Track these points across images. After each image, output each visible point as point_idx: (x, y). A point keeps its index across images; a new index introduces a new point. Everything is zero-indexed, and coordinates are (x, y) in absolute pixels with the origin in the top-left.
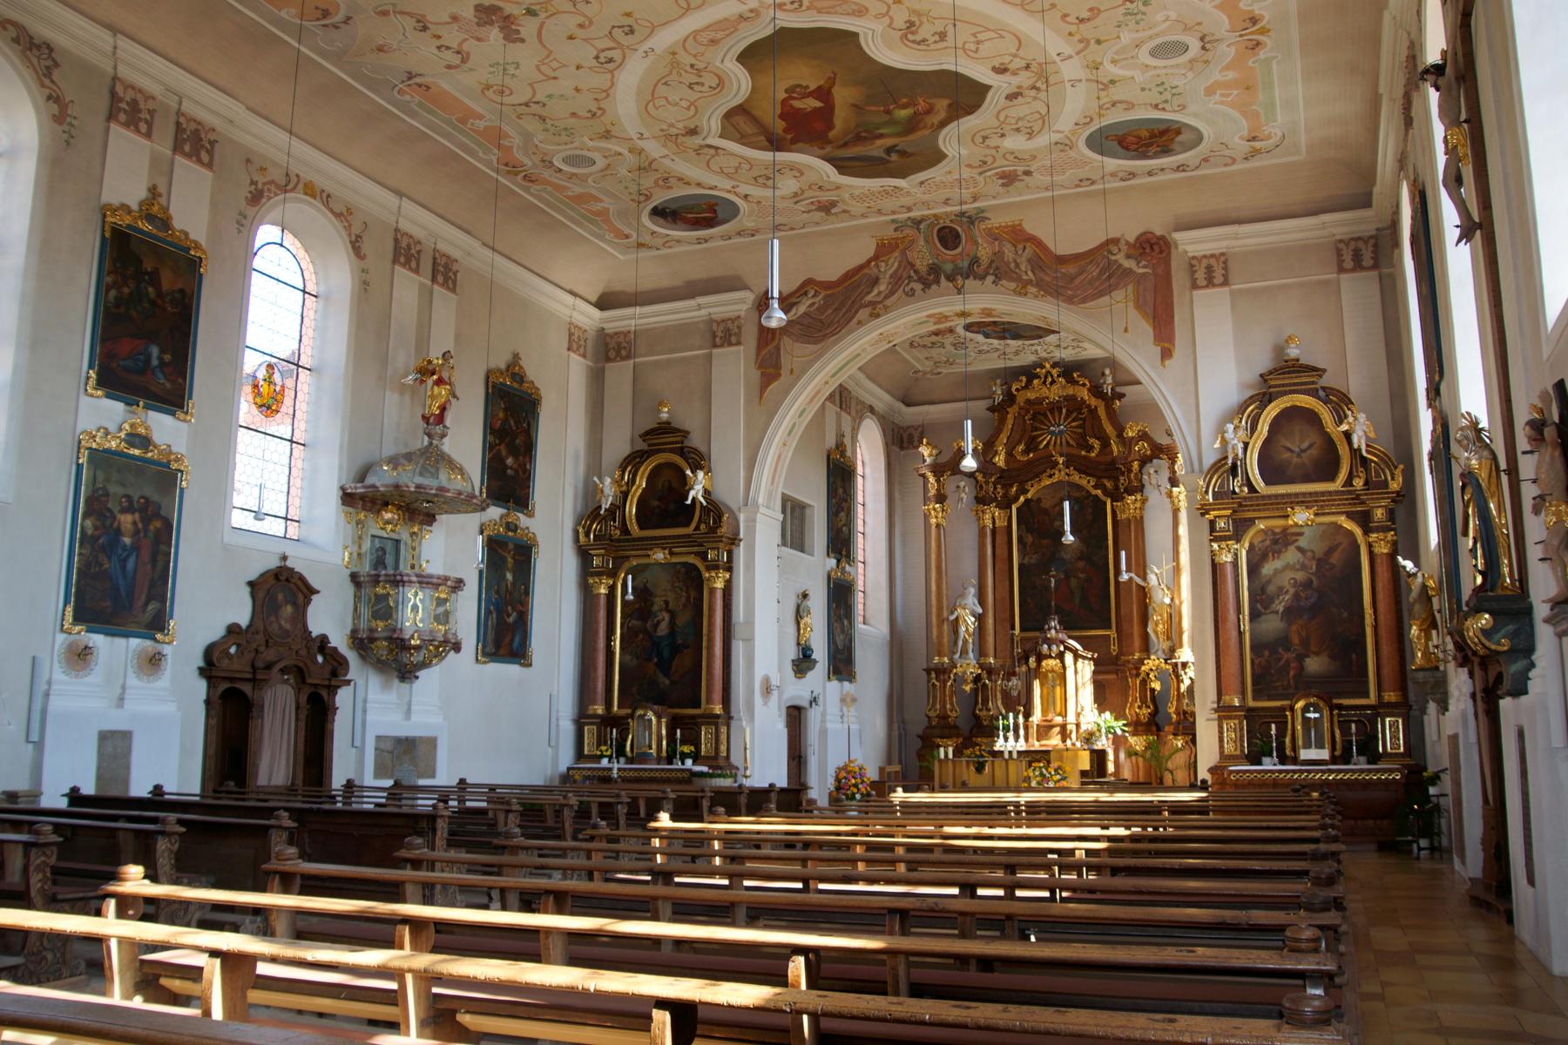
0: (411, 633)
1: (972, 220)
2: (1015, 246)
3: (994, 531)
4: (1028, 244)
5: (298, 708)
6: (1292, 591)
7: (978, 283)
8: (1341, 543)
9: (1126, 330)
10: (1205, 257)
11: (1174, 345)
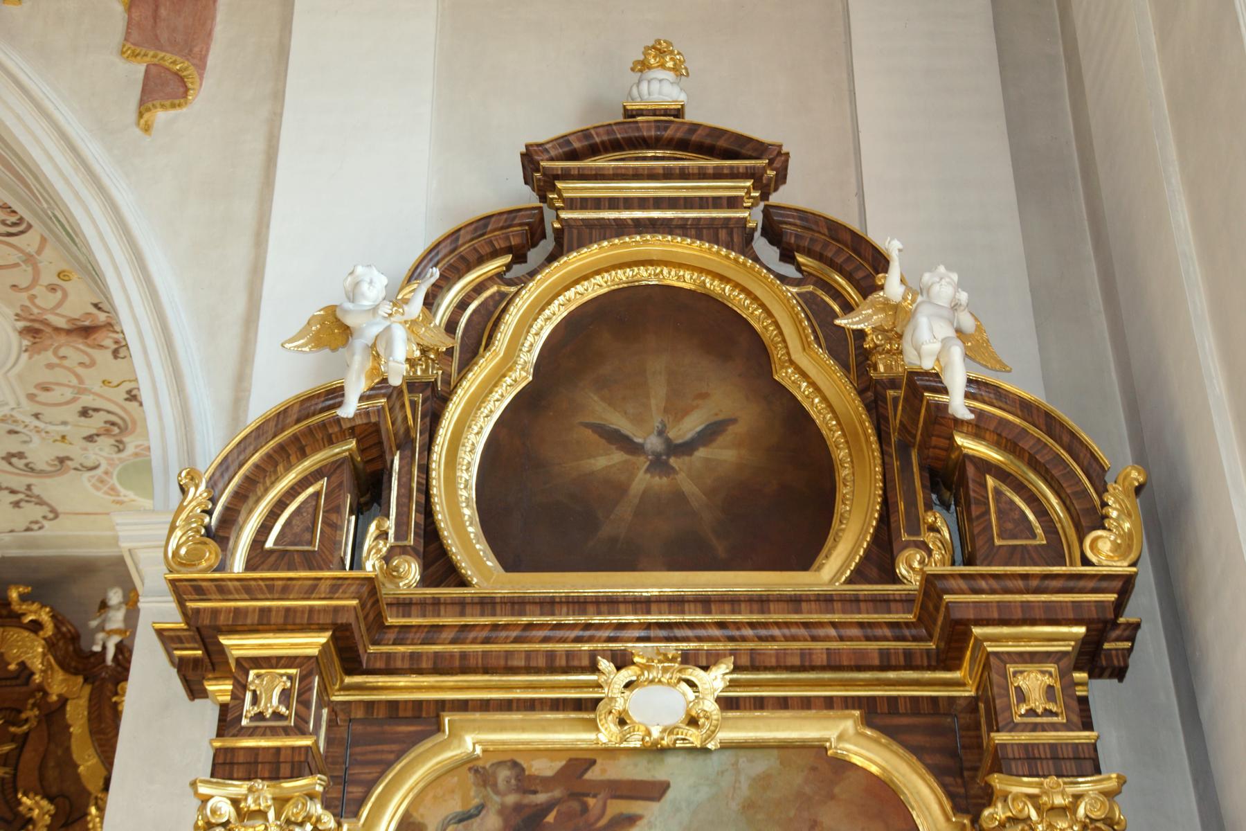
11: (201, 66)
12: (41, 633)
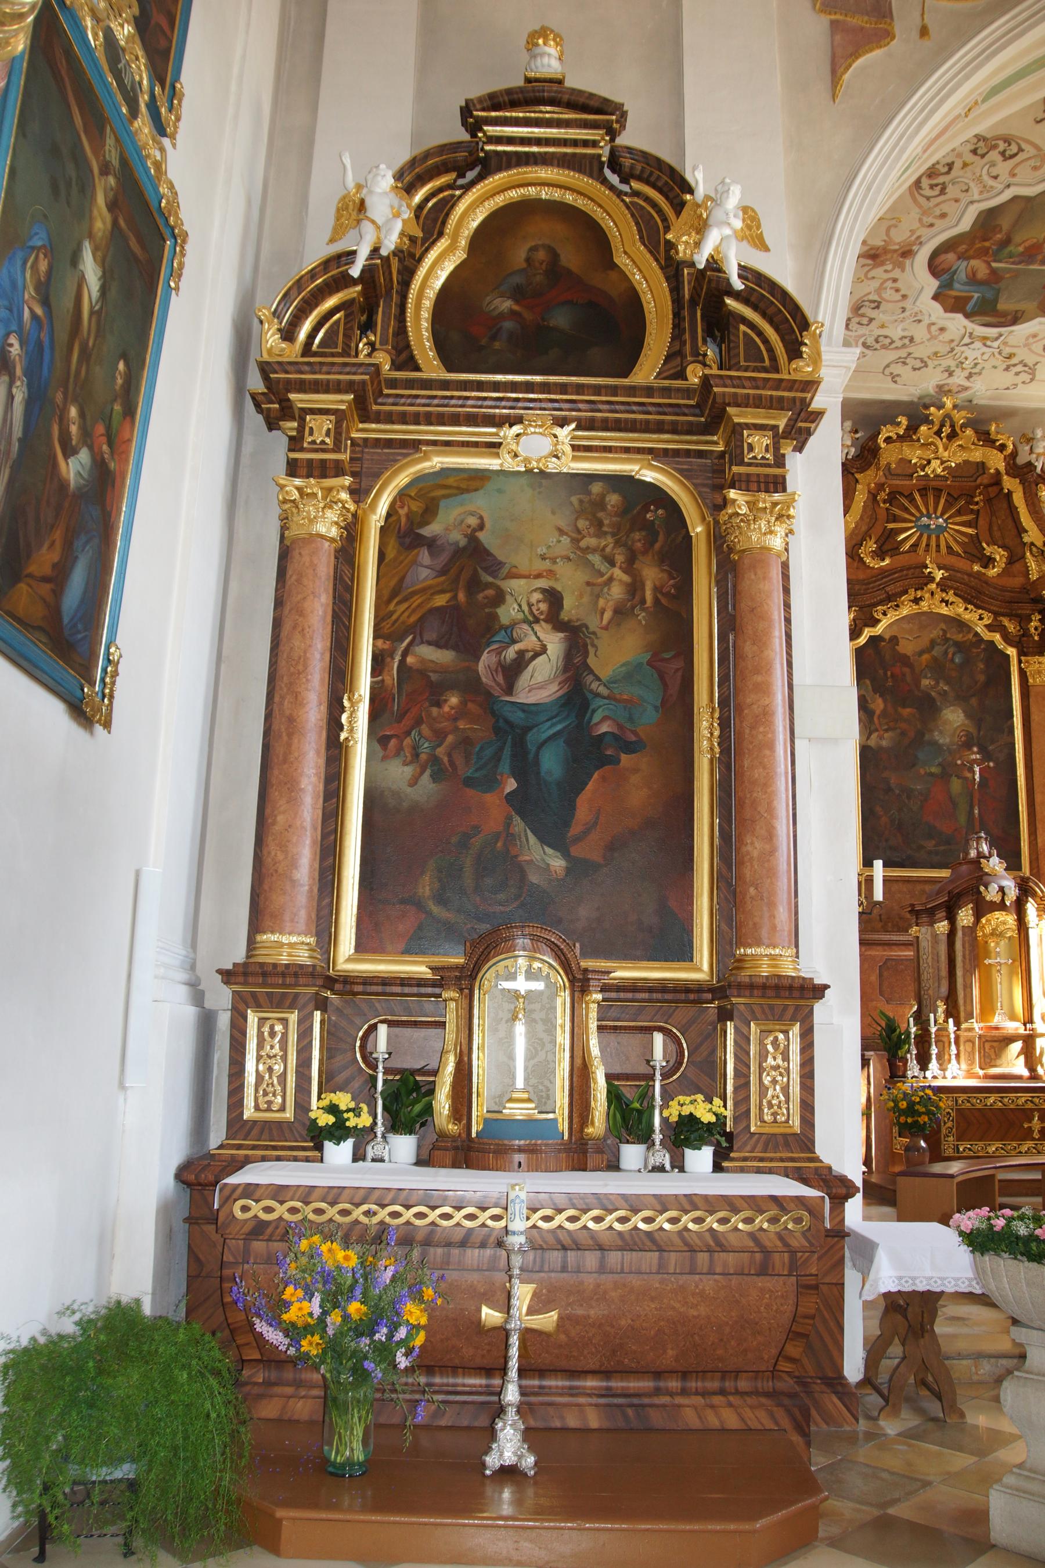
12: (1005, 453)
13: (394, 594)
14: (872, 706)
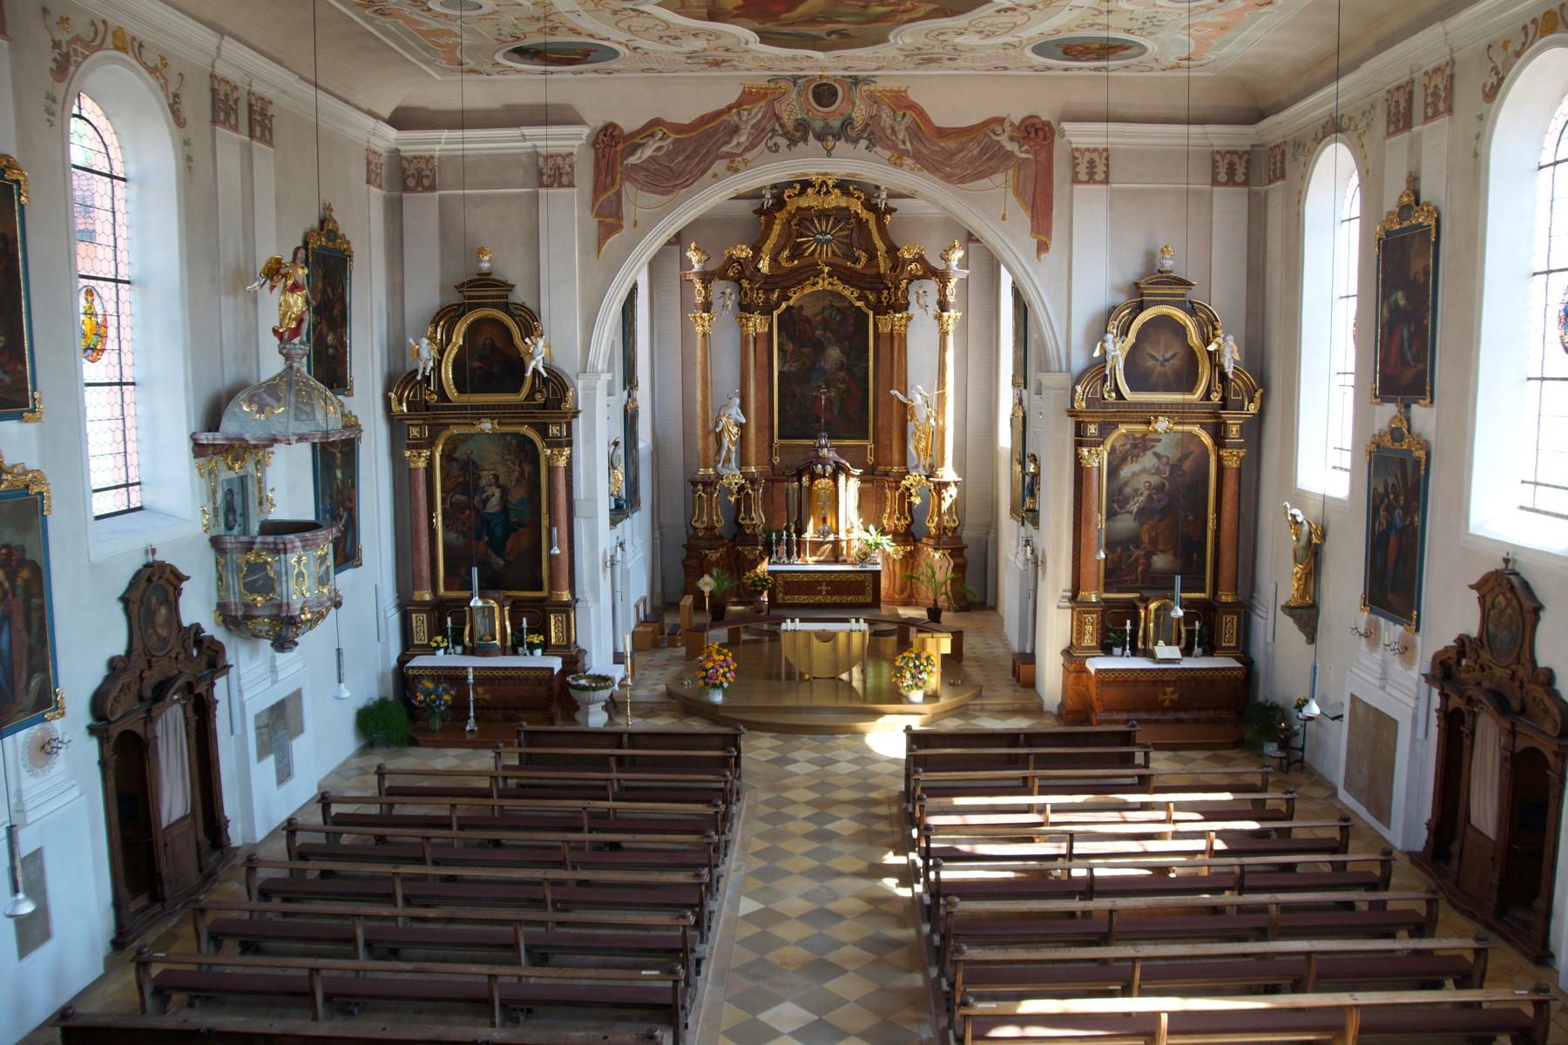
0: (299, 606)
1: (856, 81)
2: (894, 112)
3: (755, 339)
4: (909, 113)
5: (187, 724)
6: (1146, 493)
7: (850, 146)
8: (1190, 453)
9: (1003, 218)
10: (1088, 150)
13: (448, 476)
14: (786, 348)
